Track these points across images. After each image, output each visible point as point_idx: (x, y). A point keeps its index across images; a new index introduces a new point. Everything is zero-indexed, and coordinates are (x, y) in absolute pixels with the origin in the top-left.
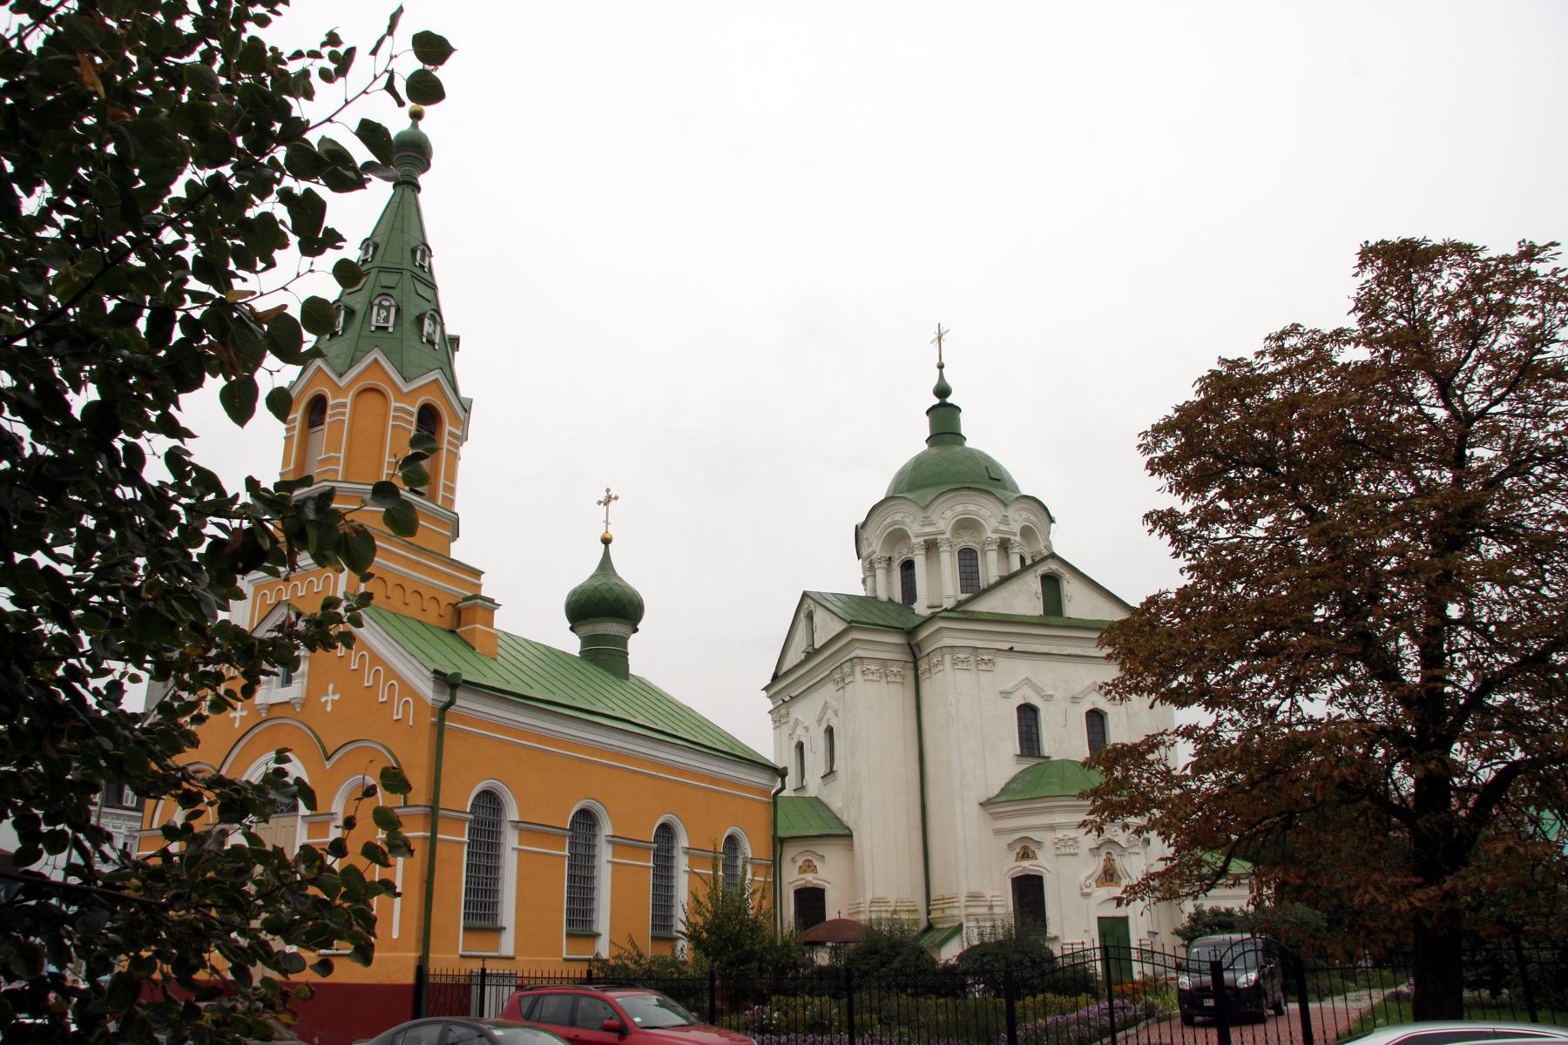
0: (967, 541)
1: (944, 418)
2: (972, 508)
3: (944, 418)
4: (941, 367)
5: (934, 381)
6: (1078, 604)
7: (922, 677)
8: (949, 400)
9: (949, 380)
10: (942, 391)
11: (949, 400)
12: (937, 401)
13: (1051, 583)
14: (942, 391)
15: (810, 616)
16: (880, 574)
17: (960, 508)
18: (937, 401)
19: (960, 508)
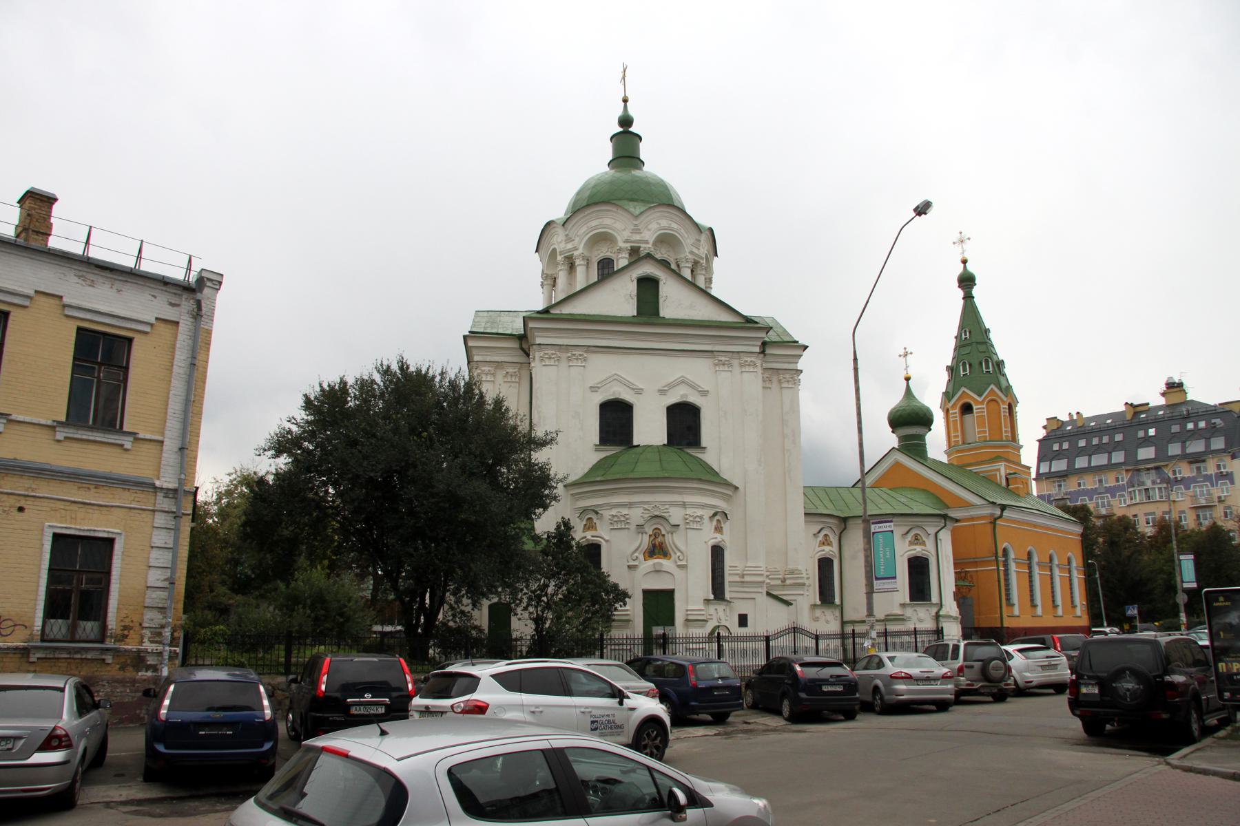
1: (626, 144)
4: (625, 101)
9: (631, 112)
10: (626, 121)
14: (626, 121)
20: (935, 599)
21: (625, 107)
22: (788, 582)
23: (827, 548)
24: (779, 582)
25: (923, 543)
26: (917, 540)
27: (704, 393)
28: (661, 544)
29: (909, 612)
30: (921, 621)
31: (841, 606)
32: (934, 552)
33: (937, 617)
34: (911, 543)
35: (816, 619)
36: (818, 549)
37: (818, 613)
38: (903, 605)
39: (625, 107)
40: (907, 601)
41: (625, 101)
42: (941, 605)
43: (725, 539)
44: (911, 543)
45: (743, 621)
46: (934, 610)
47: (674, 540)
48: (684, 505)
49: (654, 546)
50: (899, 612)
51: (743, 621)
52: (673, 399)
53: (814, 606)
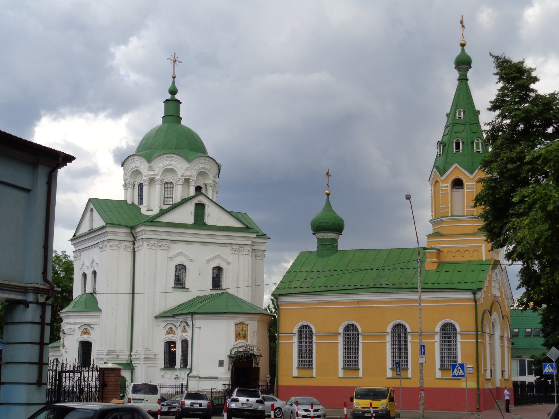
0: (169, 178)
1: (173, 106)
2: (173, 163)
3: (173, 106)
4: (174, 78)
5: (169, 85)
6: (213, 216)
8: (177, 97)
11: (177, 97)
12: (169, 96)
13: (200, 207)
14: (173, 92)
16: (130, 190)
17: (167, 163)
18: (169, 96)
19: (167, 163)
23: (170, 336)
25: (186, 332)
37: (163, 373)
41: (174, 78)
42: (191, 370)
46: (188, 372)
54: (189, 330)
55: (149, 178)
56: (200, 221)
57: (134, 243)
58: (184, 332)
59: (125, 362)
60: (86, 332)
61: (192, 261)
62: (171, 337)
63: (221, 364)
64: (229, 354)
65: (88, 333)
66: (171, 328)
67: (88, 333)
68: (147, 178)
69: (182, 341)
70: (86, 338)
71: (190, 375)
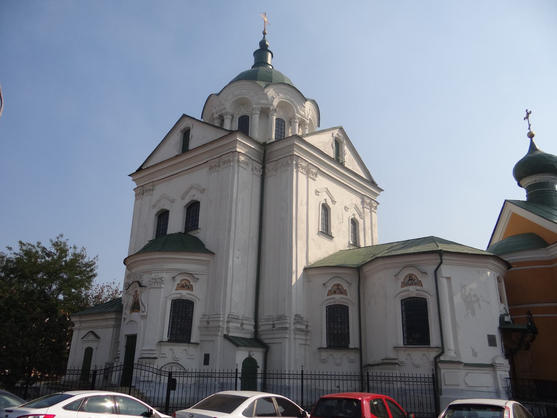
7: (268, 174)
15: (186, 134)
20: (434, 340)
21: (264, 37)
22: (277, 326)
23: (337, 296)
24: (271, 327)
25: (420, 283)
26: (411, 280)
27: (203, 191)
28: (138, 301)
29: (402, 356)
30: (417, 366)
31: (360, 350)
32: (433, 291)
33: (436, 362)
34: (404, 284)
35: (324, 361)
36: (326, 297)
37: (324, 355)
38: (396, 348)
39: (264, 37)
40: (401, 343)
42: (442, 350)
43: (198, 294)
44: (404, 284)
45: (207, 359)
46: (433, 354)
47: (143, 298)
48: (149, 272)
49: (135, 302)
50: (392, 355)
51: (207, 359)
52: (187, 201)
53: (320, 349)
54: (428, 284)
55: (261, 108)
56: (338, 159)
57: (264, 168)
58: (410, 285)
59: (249, 336)
60: (186, 286)
61: (334, 202)
62: (338, 299)
63: (492, 341)
64: (497, 324)
65: (189, 287)
66: (338, 285)
67: (189, 287)
68: (259, 107)
69: (402, 301)
70: (185, 294)
71: (442, 358)
